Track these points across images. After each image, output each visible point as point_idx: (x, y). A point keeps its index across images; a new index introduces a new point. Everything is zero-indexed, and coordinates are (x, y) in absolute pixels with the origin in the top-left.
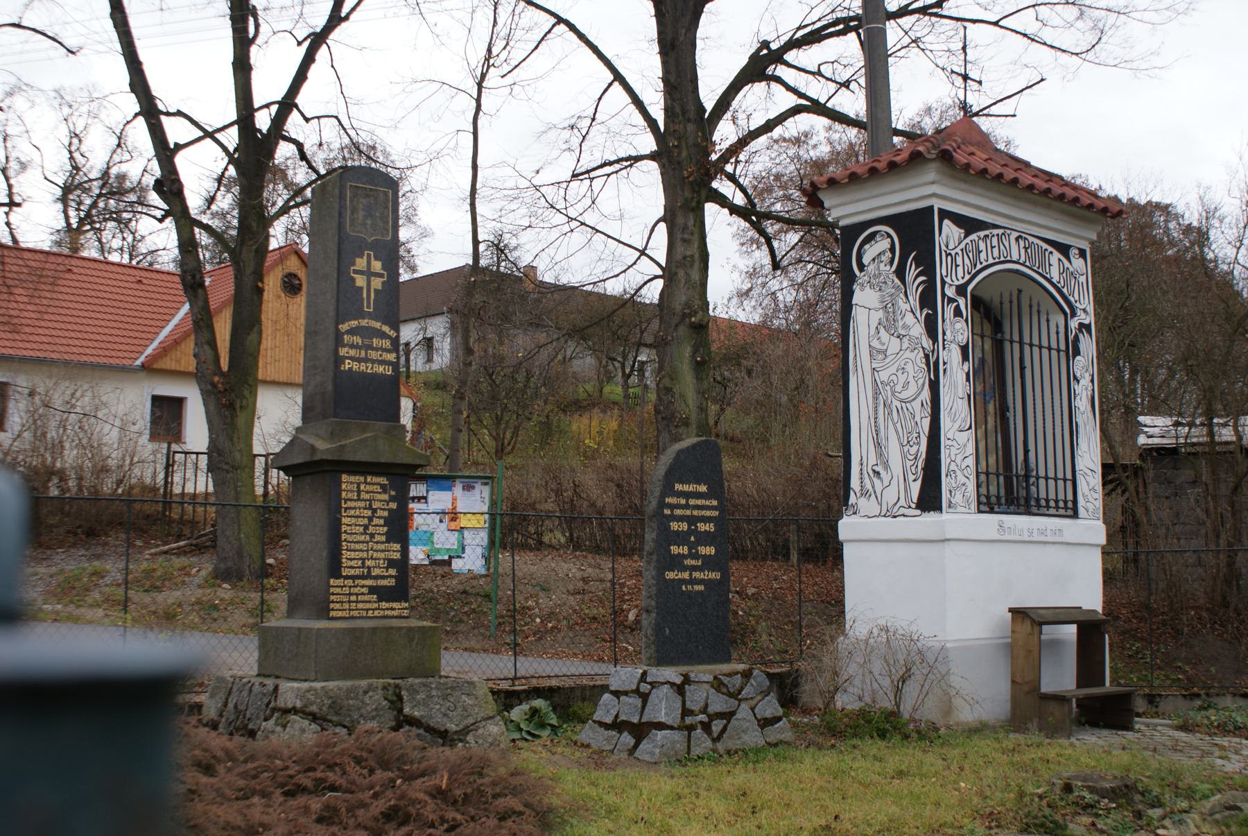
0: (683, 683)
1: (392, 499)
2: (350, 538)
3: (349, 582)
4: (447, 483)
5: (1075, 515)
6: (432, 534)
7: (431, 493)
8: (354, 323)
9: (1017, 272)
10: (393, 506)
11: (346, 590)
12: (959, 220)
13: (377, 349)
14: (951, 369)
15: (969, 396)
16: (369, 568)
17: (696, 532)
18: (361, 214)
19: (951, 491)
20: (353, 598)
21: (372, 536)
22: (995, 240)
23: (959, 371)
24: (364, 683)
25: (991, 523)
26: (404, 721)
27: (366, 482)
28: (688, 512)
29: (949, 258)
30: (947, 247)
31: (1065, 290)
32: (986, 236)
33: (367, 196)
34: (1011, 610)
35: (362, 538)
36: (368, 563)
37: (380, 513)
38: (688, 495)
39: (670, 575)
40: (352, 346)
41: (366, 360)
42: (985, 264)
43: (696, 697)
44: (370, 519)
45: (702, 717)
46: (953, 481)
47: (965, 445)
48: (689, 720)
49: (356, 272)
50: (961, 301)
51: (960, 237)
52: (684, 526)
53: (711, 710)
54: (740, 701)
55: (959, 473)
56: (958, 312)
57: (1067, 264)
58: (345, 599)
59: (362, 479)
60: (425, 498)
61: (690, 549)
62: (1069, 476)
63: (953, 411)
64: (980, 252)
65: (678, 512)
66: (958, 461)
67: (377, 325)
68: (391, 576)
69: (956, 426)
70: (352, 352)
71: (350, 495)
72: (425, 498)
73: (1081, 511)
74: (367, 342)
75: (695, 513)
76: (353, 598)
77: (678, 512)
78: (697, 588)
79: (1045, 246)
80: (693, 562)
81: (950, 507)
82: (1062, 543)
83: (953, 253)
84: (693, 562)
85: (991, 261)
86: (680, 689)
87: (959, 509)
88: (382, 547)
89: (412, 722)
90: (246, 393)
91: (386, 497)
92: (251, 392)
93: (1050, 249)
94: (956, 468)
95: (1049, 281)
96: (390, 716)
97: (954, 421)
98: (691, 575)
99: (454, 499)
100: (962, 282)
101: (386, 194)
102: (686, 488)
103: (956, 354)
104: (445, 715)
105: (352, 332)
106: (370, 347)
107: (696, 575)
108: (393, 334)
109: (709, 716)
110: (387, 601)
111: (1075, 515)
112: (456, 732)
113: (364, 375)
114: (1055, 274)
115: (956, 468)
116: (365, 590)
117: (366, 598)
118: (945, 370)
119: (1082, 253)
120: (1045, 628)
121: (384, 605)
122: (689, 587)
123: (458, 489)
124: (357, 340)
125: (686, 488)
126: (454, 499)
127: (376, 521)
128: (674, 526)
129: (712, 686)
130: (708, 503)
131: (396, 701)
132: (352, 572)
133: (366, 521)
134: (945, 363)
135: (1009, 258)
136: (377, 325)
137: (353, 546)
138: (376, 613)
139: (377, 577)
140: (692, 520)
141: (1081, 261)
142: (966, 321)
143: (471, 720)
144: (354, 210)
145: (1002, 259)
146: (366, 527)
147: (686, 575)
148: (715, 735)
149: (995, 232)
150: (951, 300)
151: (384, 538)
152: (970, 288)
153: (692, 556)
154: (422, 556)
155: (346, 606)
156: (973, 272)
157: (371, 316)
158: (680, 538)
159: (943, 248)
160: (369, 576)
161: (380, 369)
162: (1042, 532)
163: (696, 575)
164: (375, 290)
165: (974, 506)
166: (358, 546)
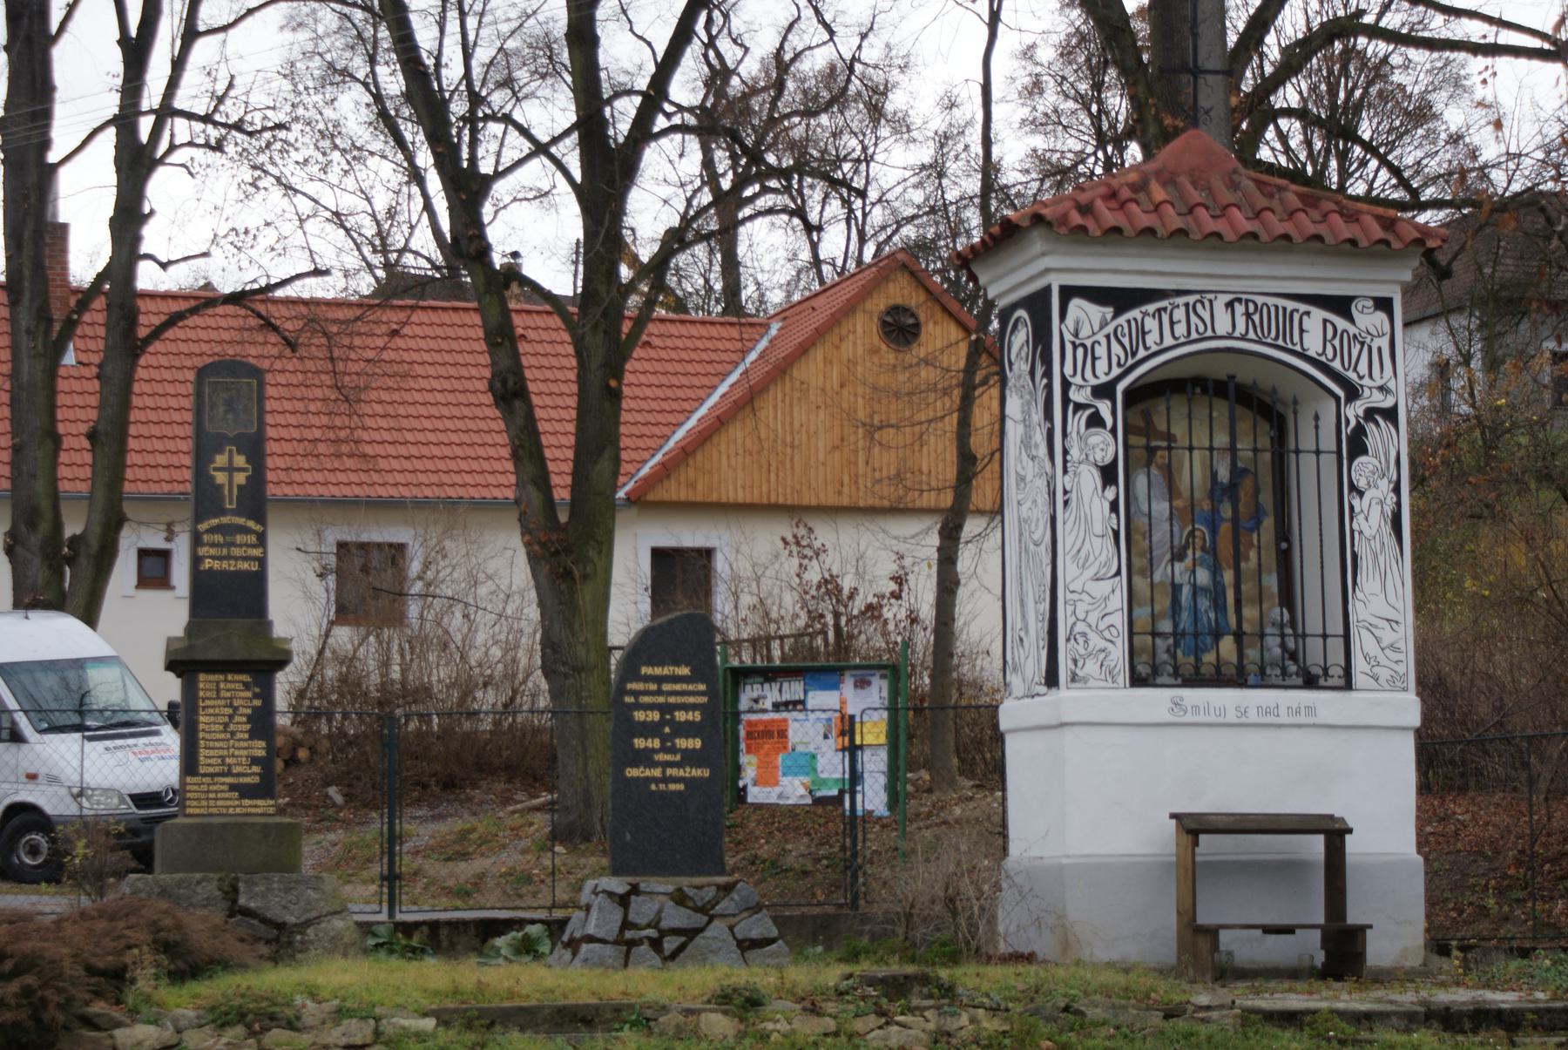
0: (628, 894)
1: (256, 696)
2: (208, 736)
3: (208, 780)
4: (833, 678)
5: (1348, 684)
6: (814, 757)
7: (810, 694)
8: (214, 522)
10: (258, 703)
11: (204, 788)
12: (1097, 295)
13: (240, 546)
14: (1080, 499)
15: (1116, 534)
16: (230, 766)
17: (673, 723)
18: (222, 409)
20: (212, 795)
21: (233, 733)
22: (1179, 314)
23: (1096, 501)
24: (198, 876)
25: (1157, 701)
26: (235, 910)
27: (226, 681)
28: (661, 700)
30: (1076, 335)
31: (1336, 365)
32: (1159, 310)
33: (228, 389)
34: (1173, 816)
35: (222, 736)
36: (228, 761)
37: (242, 710)
38: (659, 680)
39: (632, 772)
40: (212, 545)
41: (228, 558)
42: (1154, 348)
43: (642, 910)
44: (231, 717)
45: (652, 933)
48: (629, 935)
49: (216, 469)
51: (1104, 317)
52: (655, 716)
53: (664, 924)
54: (711, 919)
55: (1092, 636)
56: (1095, 421)
57: (1341, 323)
58: (203, 796)
59: (222, 677)
60: (802, 702)
61: (663, 742)
62: (1336, 627)
63: (1083, 554)
64: (1144, 333)
65: (646, 699)
66: (1092, 619)
67: (241, 521)
68: (254, 774)
70: (213, 551)
71: (208, 694)
72: (802, 702)
73: (1359, 679)
74: (229, 539)
75: (672, 700)
76: (212, 795)
77: (646, 699)
78: (672, 787)
79: (1291, 305)
80: (668, 757)
81: (1073, 680)
82: (1314, 726)
83: (1088, 343)
84: (668, 757)
85: (1168, 341)
86: (623, 901)
87: (1091, 683)
88: (245, 744)
89: (246, 912)
90: (592, 554)
91: (249, 694)
92: (600, 552)
93: (1303, 307)
94: (1087, 630)
95: (1302, 356)
96: (226, 905)
98: (664, 772)
99: (843, 702)
100: (1103, 379)
101: (249, 384)
102: (658, 671)
103: (1089, 479)
104: (284, 907)
105: (212, 530)
106: (234, 544)
107: (670, 772)
108: (258, 528)
109: (660, 931)
110: (250, 798)
111: (1348, 684)
112: (296, 925)
113: (223, 573)
114: (1313, 344)
115: (1087, 630)
116: (225, 788)
117: (227, 795)
118: (1066, 503)
119: (1384, 304)
120: (1203, 838)
121: (247, 802)
122: (662, 787)
123: (848, 686)
124: (219, 538)
125: (658, 671)
126: (843, 702)
127: (237, 719)
128: (639, 716)
129: (672, 899)
130: (691, 687)
131: (232, 893)
132: (211, 770)
133: (226, 719)
134: (1065, 492)
135: (1209, 333)
136: (241, 521)
137: (212, 744)
138: (238, 810)
139: (239, 775)
140: (665, 709)
141: (1380, 317)
142: (1114, 431)
143: (314, 914)
144: (213, 406)
145: (1194, 336)
146: (226, 725)
147: (657, 772)
148: (667, 953)
149: (1181, 300)
150: (1079, 407)
151: (246, 736)
152: (1121, 387)
153: (663, 749)
154: (802, 791)
155: (204, 803)
156: (1130, 362)
157: (234, 513)
158: (648, 730)
159: (1068, 337)
160: (229, 774)
161: (244, 566)
163: (670, 772)
164: (240, 487)
165: (1123, 677)
166: (217, 744)
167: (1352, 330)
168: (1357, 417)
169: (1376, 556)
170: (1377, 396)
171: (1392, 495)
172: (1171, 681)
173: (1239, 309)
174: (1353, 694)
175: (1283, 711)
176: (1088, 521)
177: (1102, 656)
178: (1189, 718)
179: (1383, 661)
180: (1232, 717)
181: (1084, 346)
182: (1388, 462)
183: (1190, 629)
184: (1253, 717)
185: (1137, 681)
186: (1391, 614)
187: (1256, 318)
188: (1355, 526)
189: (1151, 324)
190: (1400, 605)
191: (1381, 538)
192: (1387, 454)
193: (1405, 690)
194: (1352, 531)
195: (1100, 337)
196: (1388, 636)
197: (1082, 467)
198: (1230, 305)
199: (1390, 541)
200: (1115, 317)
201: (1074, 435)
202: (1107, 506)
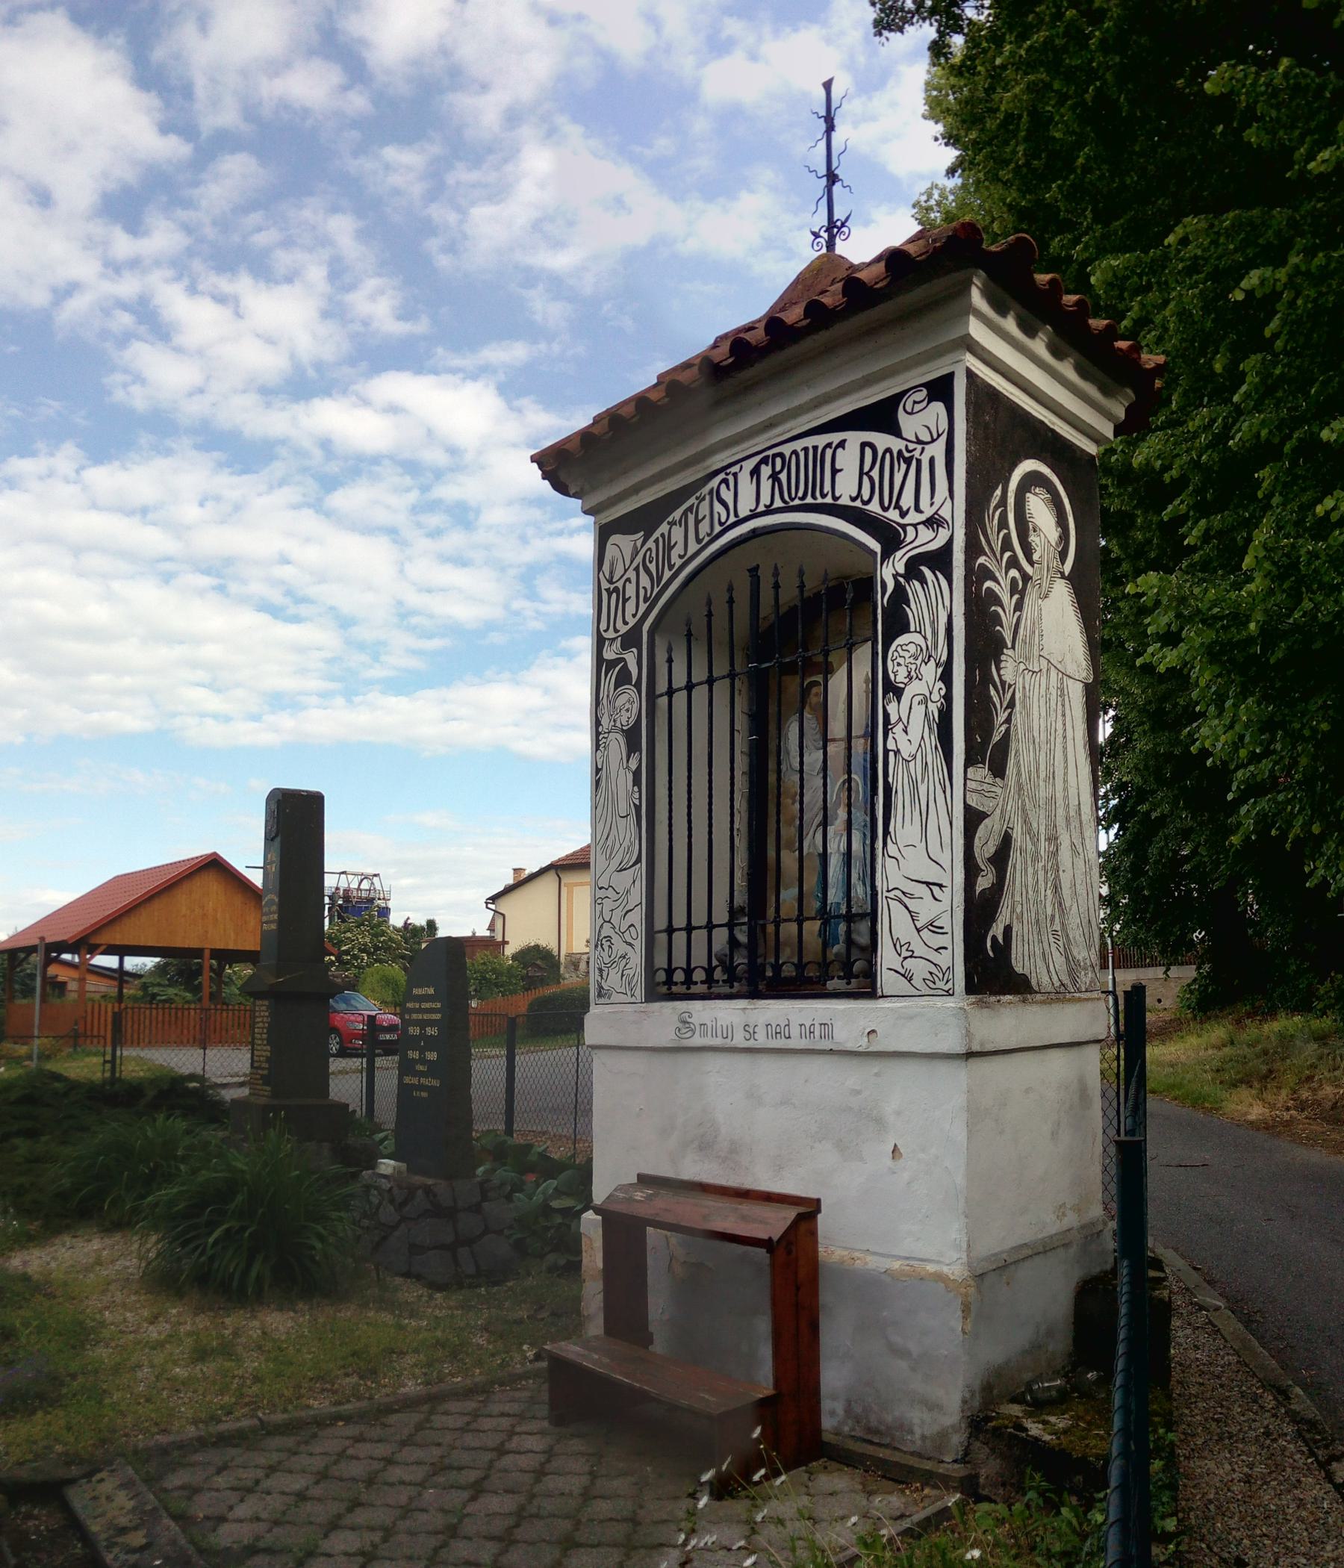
9: (755, 533)
15: (638, 808)
19: (601, 970)
31: (874, 507)
46: (605, 955)
55: (616, 939)
57: (882, 441)
64: (671, 548)
79: (821, 440)
81: (600, 995)
87: (615, 998)
94: (611, 933)
97: (610, 858)
115: (611, 933)
162: (779, 1031)
165: (639, 992)
167: (896, 444)
168: (895, 576)
170: (925, 534)
171: (940, 684)
172: (726, 990)
173: (766, 471)
174: (882, 1004)
175: (795, 1031)
176: (615, 802)
179: (919, 950)
180: (739, 1040)
182: (935, 633)
183: (704, 922)
184: (761, 1040)
185: (653, 994)
186: (933, 874)
187: (783, 477)
188: (891, 745)
189: (677, 534)
190: (944, 859)
191: (924, 757)
192: (934, 623)
193: (949, 993)
194: (886, 752)
198: (755, 472)
199: (935, 759)
202: (630, 777)
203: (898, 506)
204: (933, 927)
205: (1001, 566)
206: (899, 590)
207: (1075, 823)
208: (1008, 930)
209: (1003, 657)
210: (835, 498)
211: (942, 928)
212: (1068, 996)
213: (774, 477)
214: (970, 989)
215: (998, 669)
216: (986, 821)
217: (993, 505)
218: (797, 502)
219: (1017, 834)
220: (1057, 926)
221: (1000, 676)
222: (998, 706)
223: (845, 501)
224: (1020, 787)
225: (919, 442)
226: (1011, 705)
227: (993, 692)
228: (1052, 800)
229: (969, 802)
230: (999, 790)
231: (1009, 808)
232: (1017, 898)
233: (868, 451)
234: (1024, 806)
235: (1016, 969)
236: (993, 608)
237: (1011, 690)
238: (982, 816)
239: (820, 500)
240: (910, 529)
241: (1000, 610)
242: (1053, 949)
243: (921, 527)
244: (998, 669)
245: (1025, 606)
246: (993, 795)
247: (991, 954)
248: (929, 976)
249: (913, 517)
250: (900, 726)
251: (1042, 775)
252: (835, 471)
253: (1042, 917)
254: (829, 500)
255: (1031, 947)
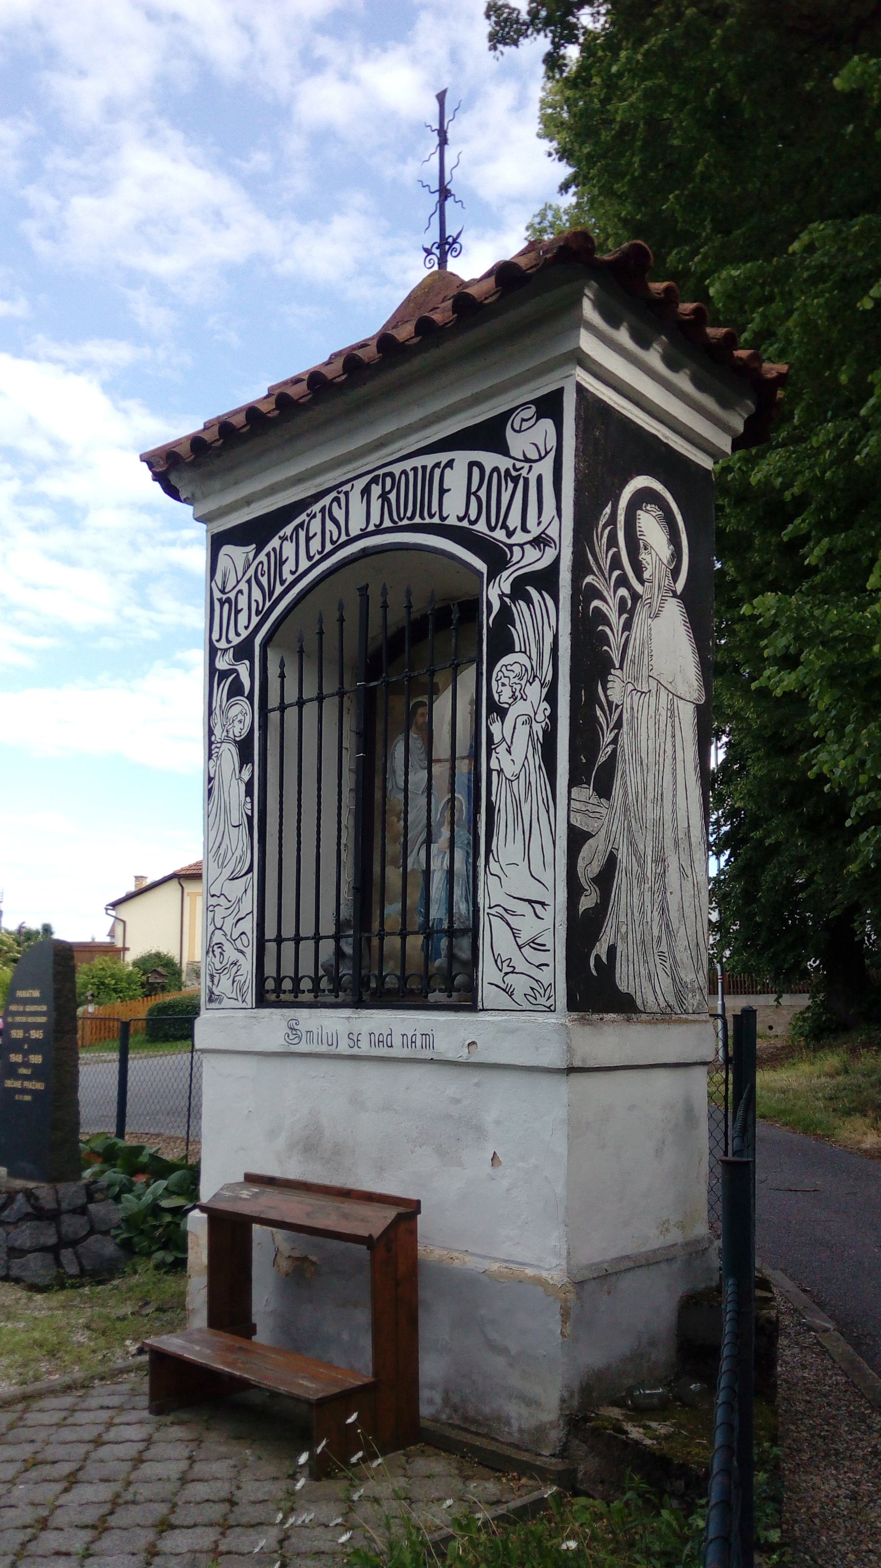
9: (365, 553)
15: (250, 819)
19: (212, 976)
23: (234, 782)
29: (226, 606)
31: (481, 527)
46: (216, 961)
47: (240, 900)
50: (243, 669)
51: (247, 559)
55: (227, 946)
57: (490, 460)
63: (222, 851)
64: (282, 563)
69: (227, 872)
77: (18, 1019)
79: (429, 460)
81: (211, 1000)
83: (232, 595)
87: (226, 1003)
94: (222, 939)
97: (223, 866)
115: (222, 939)
140: (27, 1027)
142: (250, 698)
165: (250, 998)
167: (504, 463)
168: (501, 596)
169: (518, 806)
170: (532, 553)
171: (545, 705)
172: (331, 999)
173: (376, 490)
175: (397, 1040)
176: (227, 811)
177: (235, 968)
178: (303, 1047)
180: (343, 1048)
181: (228, 600)
182: (540, 654)
183: (311, 933)
184: (365, 1048)
185: (262, 1001)
187: (392, 496)
188: (494, 765)
189: (289, 549)
190: (548, 879)
191: (528, 776)
192: (539, 642)
193: (551, 1010)
194: (489, 771)
195: (243, 586)
196: (528, 927)
197: (225, 746)
198: (366, 492)
199: (539, 779)
200: (255, 557)
201: (218, 711)
202: (243, 787)
203: (504, 526)
204: (535, 945)
205: (609, 585)
206: (506, 611)
207: (684, 845)
208: (612, 950)
209: (610, 678)
210: (443, 518)
211: (544, 945)
212: (674, 1017)
213: (384, 496)
214: (572, 1006)
215: (605, 689)
216: (591, 841)
217: (601, 523)
218: (405, 522)
219: (622, 855)
220: (664, 948)
221: (606, 696)
222: (605, 727)
223: (452, 521)
224: (626, 809)
225: (527, 460)
226: (619, 725)
227: (599, 712)
228: (659, 822)
229: (573, 822)
230: (604, 811)
231: (614, 828)
232: (622, 918)
233: (476, 471)
234: (630, 827)
235: (621, 988)
236: (600, 628)
237: (619, 711)
238: (587, 836)
239: (428, 520)
240: (516, 549)
241: (607, 630)
242: (660, 971)
243: (527, 547)
244: (605, 689)
245: (634, 626)
246: (598, 815)
247: (594, 973)
248: (530, 992)
249: (520, 537)
250: (504, 745)
251: (650, 796)
252: (443, 491)
253: (648, 938)
254: (436, 520)
255: (636, 967)
